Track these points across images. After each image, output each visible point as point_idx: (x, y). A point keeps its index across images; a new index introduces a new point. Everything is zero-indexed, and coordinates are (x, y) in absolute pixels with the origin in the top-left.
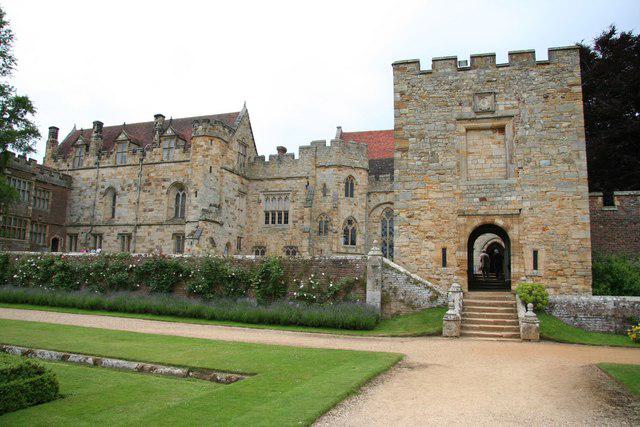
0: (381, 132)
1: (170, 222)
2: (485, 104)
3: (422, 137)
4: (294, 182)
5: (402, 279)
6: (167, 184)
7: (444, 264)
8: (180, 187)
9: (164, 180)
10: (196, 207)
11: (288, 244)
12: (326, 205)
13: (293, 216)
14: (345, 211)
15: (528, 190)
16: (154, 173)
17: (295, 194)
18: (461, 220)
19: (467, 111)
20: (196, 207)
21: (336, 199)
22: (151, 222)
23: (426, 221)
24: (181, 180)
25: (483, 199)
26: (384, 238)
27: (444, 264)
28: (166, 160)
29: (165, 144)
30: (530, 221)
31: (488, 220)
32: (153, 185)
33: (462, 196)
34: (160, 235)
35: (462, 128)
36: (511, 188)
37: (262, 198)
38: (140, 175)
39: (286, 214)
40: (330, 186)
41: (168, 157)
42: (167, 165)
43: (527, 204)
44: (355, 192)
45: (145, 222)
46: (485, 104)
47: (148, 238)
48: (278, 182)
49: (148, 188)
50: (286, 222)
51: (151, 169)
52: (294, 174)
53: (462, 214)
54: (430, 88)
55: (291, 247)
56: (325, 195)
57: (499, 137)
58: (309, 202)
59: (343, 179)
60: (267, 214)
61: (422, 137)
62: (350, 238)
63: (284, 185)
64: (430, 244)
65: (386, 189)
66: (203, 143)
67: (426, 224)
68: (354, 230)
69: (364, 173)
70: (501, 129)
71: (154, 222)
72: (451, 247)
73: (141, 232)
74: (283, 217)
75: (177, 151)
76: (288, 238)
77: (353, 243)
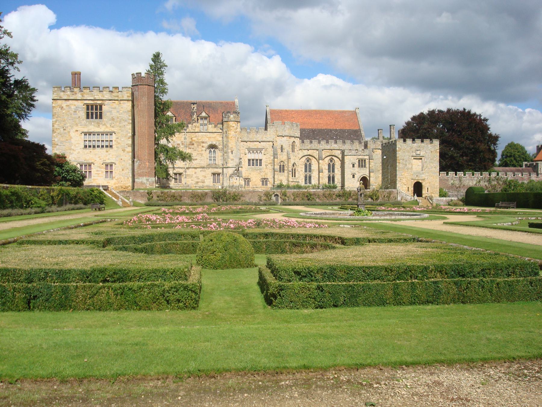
0: (293, 111)
1: (209, 166)
2: (418, 152)
3: (403, 160)
4: (264, 143)
5: (405, 195)
6: (206, 145)
7: (408, 191)
8: (213, 147)
9: (203, 142)
10: (232, 160)
11: (263, 177)
12: (283, 157)
13: (266, 162)
14: (292, 161)
15: (427, 174)
16: (196, 138)
17: (266, 150)
18: (412, 181)
19: (414, 154)
20: (232, 160)
21: (288, 154)
22: (195, 166)
23: (404, 181)
24: (214, 143)
25: (417, 176)
26: (306, 173)
27: (408, 191)
28: (202, 131)
29: (200, 121)
30: (427, 181)
31: (418, 181)
32: (195, 145)
33: (412, 175)
34: (203, 173)
35: (413, 158)
36: (423, 173)
37: (247, 152)
38: (185, 138)
39: (261, 160)
40: (284, 146)
41: (203, 129)
42: (204, 134)
43: (426, 177)
44: (295, 150)
45: (192, 167)
46: (418, 152)
47: (194, 175)
48: (255, 143)
49: (192, 147)
50: (260, 165)
51: (193, 135)
52: (264, 139)
53: (412, 179)
54: (406, 147)
55: (265, 179)
56: (282, 151)
57: (420, 160)
58: (275, 155)
59: (291, 143)
60: (249, 160)
61: (403, 160)
62: (294, 175)
63: (260, 145)
64: (405, 186)
65: (308, 148)
66: (234, 125)
67: (404, 181)
68: (295, 170)
69: (298, 139)
70: (421, 159)
71: (198, 167)
72: (410, 187)
73: (189, 172)
74: (259, 162)
75: (210, 126)
76: (263, 174)
77: (295, 177)
